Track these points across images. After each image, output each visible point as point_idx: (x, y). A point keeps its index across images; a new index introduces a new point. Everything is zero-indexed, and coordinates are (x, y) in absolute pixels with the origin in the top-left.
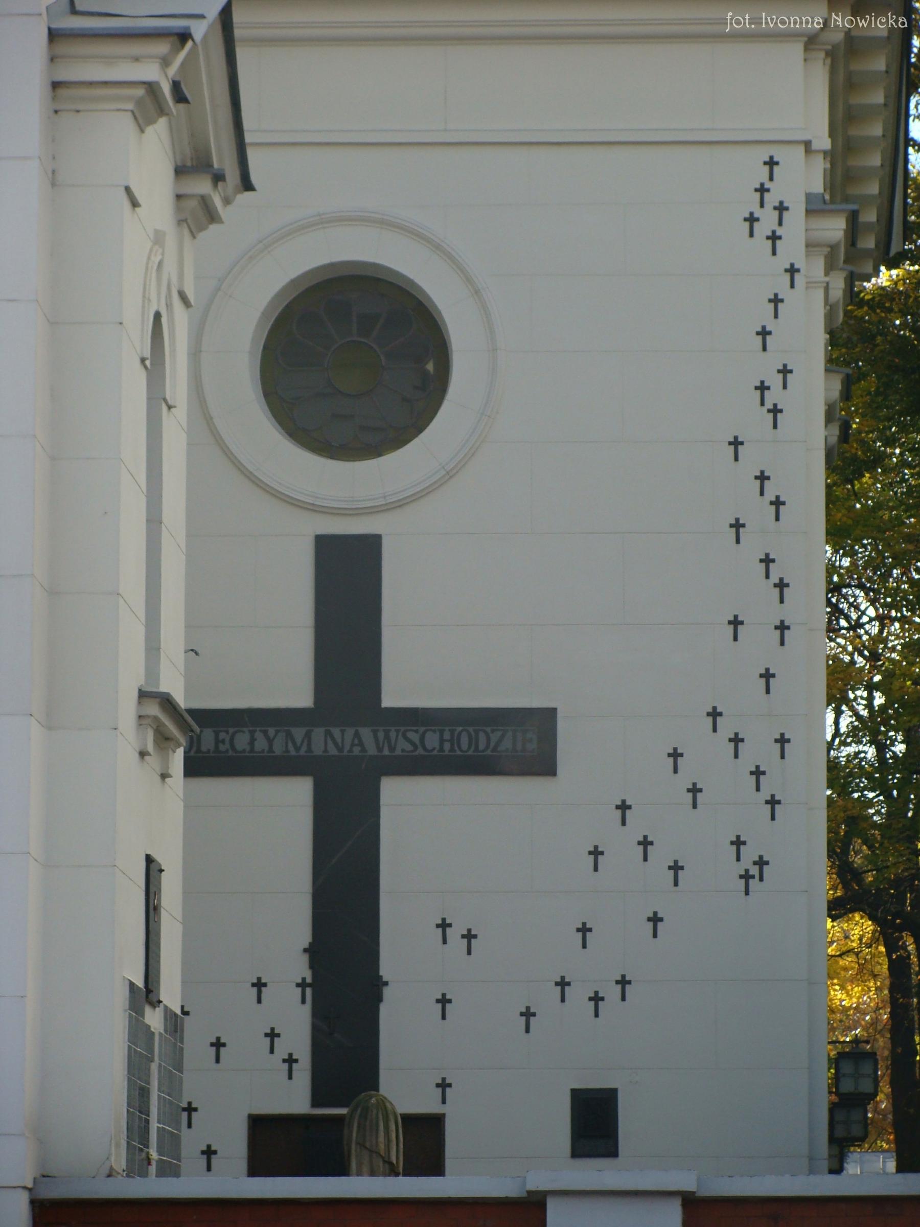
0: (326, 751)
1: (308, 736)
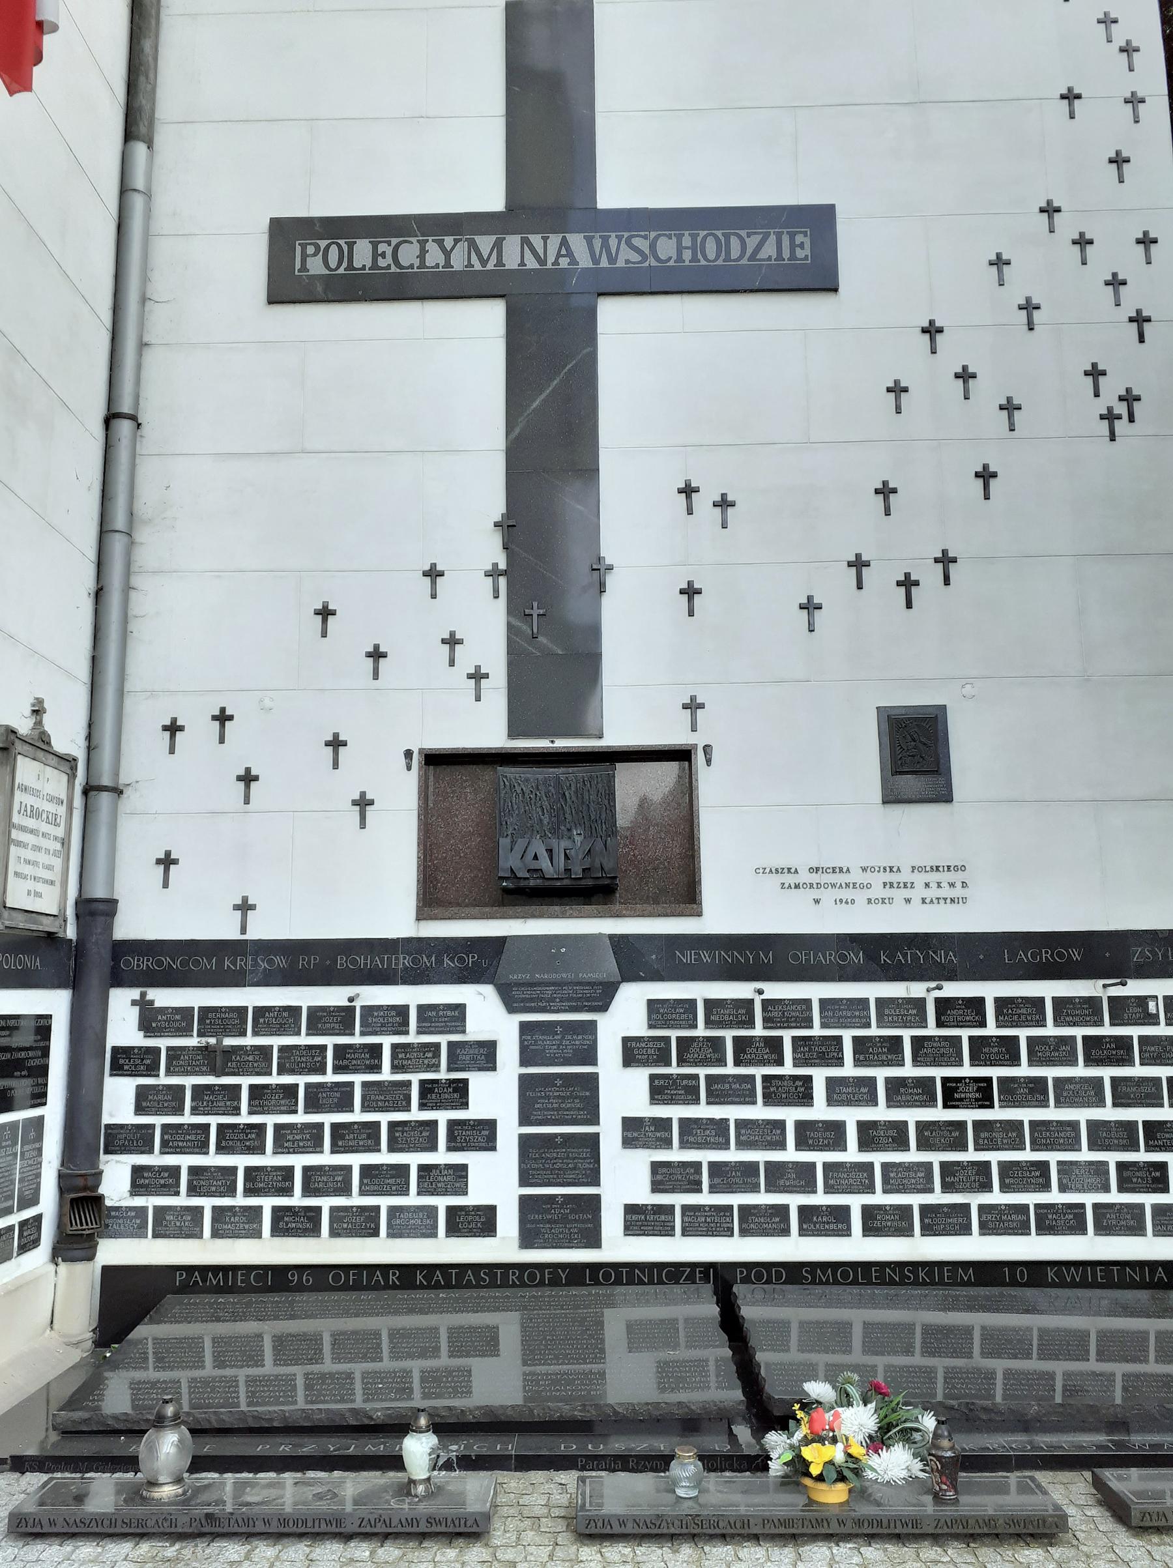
0: (522, 264)
1: (498, 245)
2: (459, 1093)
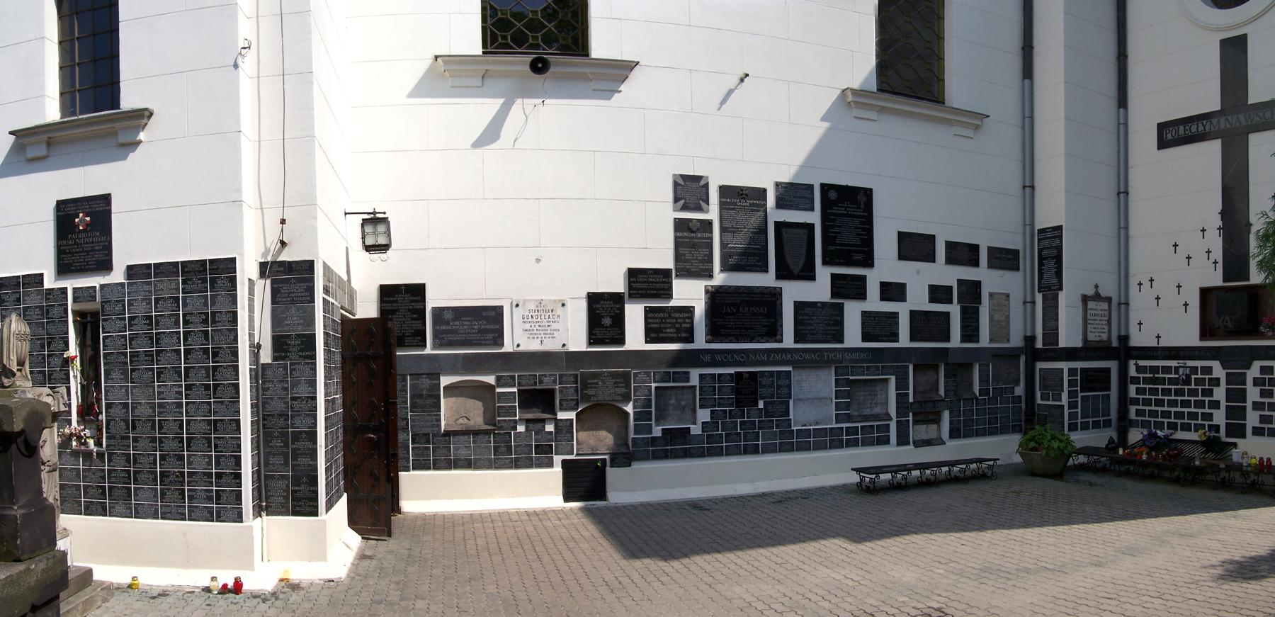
2: (1210, 393)
